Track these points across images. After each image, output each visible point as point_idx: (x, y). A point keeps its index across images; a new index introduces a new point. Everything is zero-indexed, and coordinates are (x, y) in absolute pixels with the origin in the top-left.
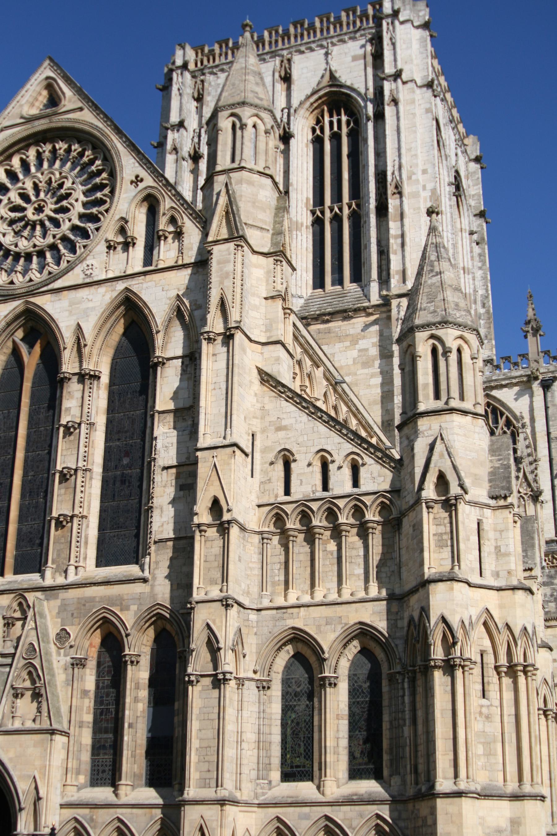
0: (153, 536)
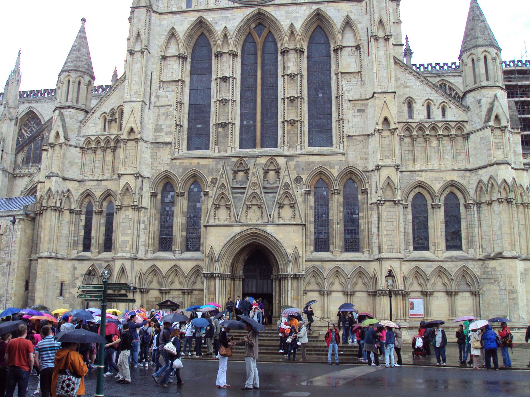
0: (345, 133)
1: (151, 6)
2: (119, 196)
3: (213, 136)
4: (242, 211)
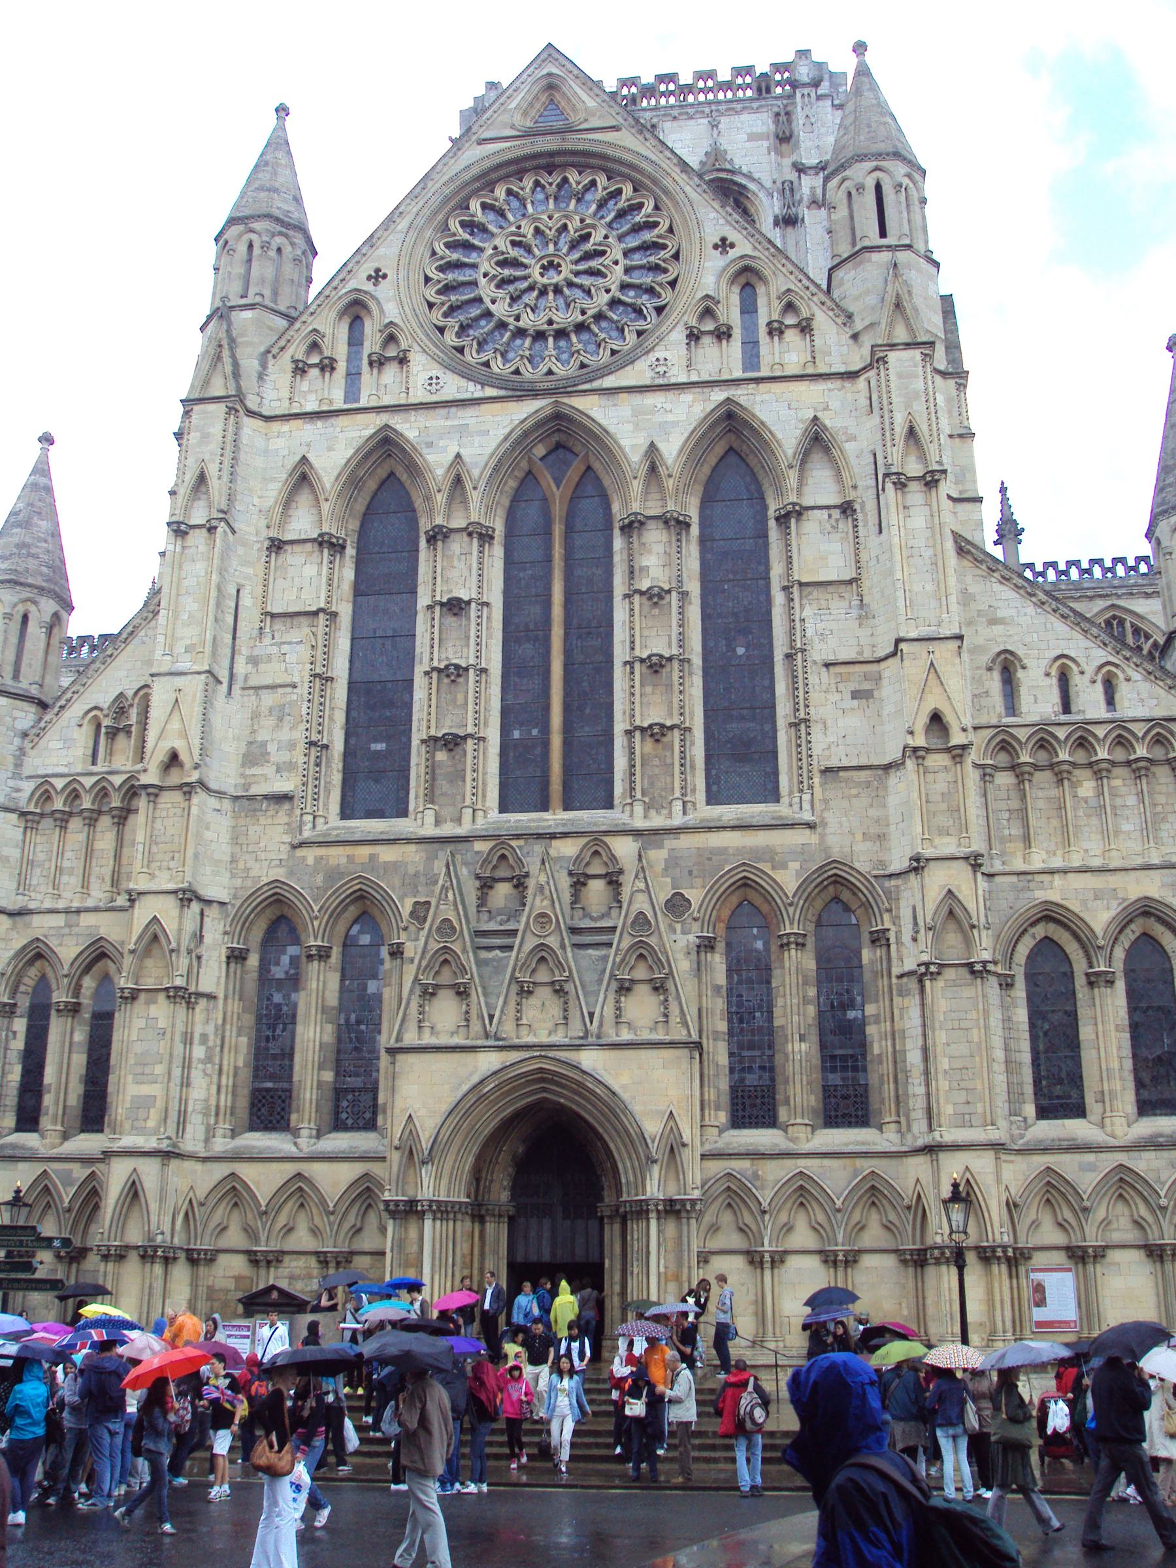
0: (815, 763)
1: (240, 397)
2: (128, 960)
3: (418, 777)
4: (505, 1003)
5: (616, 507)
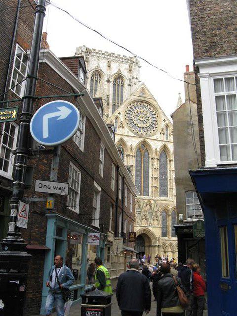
5: (150, 155)
